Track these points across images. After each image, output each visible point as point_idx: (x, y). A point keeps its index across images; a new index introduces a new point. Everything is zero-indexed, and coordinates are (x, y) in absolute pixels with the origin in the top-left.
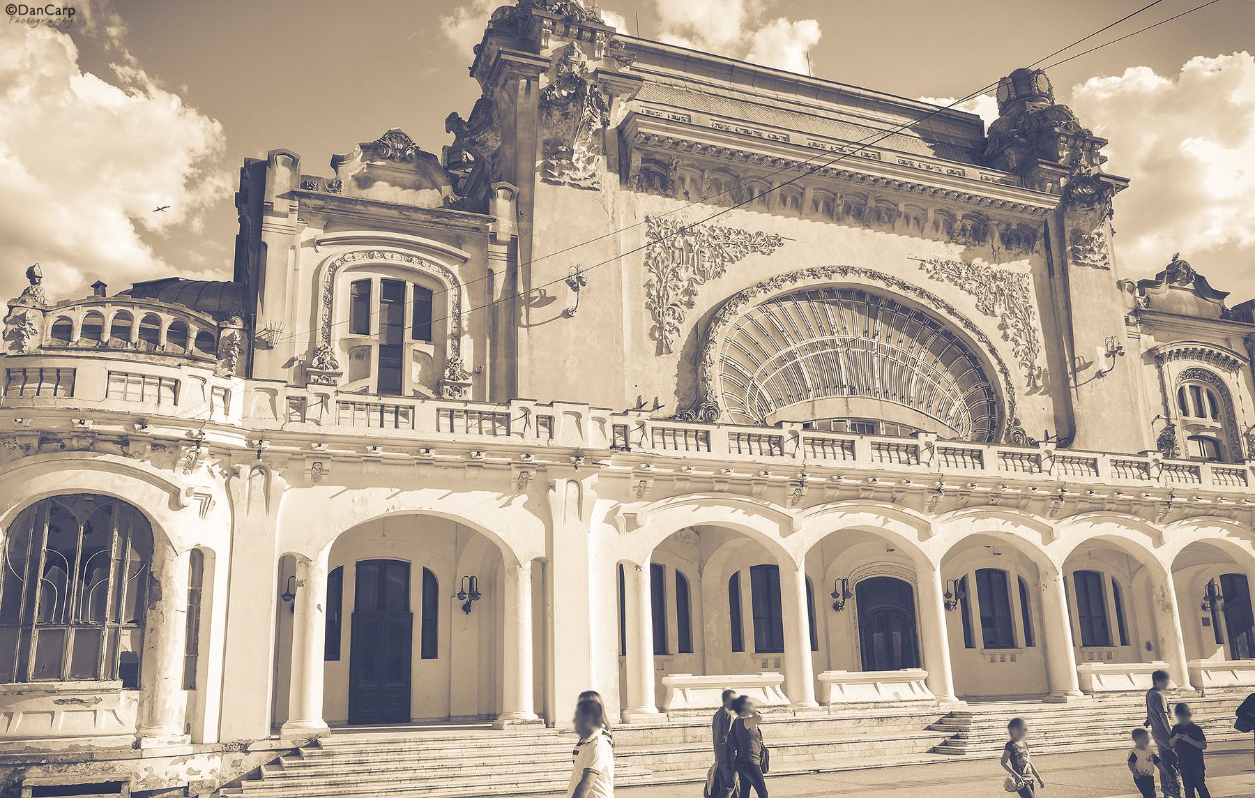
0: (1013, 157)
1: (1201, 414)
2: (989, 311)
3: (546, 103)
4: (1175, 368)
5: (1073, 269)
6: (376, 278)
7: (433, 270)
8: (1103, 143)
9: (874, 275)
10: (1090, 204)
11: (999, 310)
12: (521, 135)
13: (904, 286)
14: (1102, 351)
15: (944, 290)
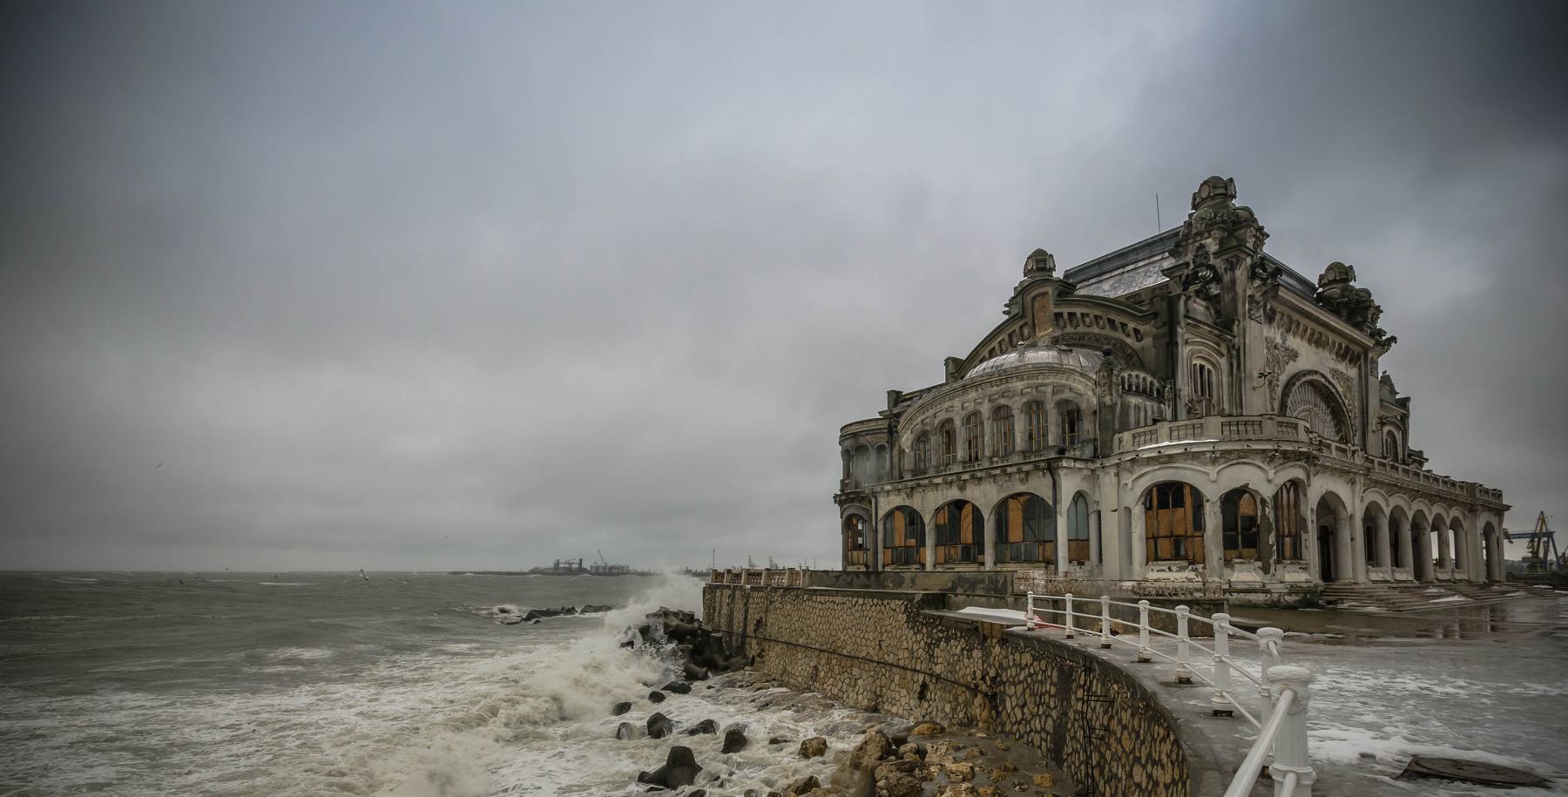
0: (1344, 312)
6: (1198, 362)
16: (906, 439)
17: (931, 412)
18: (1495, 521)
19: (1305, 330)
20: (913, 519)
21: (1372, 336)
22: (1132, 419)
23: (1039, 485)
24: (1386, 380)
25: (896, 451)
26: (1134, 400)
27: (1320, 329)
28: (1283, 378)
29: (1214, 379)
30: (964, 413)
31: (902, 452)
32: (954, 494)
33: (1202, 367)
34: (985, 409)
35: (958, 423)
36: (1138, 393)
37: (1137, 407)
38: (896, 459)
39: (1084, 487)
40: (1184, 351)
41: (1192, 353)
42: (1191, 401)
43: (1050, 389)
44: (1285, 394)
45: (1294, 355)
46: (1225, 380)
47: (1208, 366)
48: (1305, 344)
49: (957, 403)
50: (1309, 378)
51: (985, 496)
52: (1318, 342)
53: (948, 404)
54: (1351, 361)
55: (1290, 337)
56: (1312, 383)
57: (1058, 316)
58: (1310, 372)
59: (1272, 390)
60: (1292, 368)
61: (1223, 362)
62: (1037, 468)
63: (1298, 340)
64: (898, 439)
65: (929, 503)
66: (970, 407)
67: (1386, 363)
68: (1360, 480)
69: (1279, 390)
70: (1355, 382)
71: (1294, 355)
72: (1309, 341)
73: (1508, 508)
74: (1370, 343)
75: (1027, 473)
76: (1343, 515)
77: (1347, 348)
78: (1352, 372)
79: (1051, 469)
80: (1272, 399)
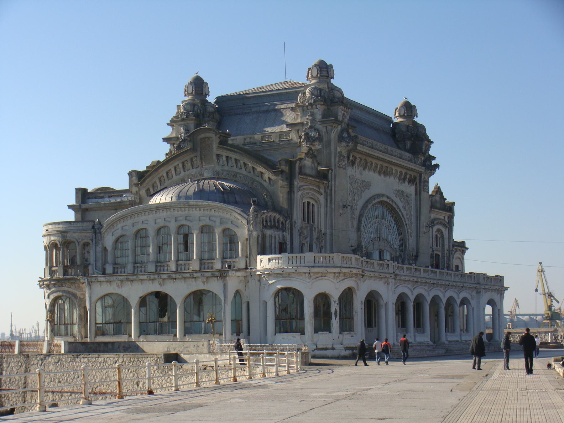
0: (408, 144)
1: (437, 246)
2: (404, 208)
3: (341, 139)
4: (435, 228)
5: (422, 192)
6: (306, 200)
7: (316, 198)
8: (433, 142)
9: (388, 197)
10: (431, 170)
11: (407, 208)
12: (332, 148)
13: (393, 201)
14: (425, 224)
15: (397, 200)
16: (109, 241)
17: (129, 222)
18: (496, 297)
19: (376, 167)
20: (122, 304)
21: (423, 164)
22: (268, 244)
23: (215, 286)
24: (438, 190)
25: (99, 249)
26: (268, 232)
27: (386, 165)
28: (360, 203)
29: (316, 210)
30: (157, 226)
31: (105, 249)
32: (155, 287)
33: (308, 203)
34: (173, 226)
35: (152, 233)
36: (271, 227)
37: (271, 236)
38: (99, 255)
39: (241, 287)
40: (298, 195)
41: (303, 197)
42: (302, 228)
43: (218, 220)
44: (361, 216)
45: (368, 185)
46: (322, 210)
47: (312, 202)
48: (376, 175)
49: (150, 218)
50: (377, 200)
51: (178, 291)
52: (385, 173)
53: (143, 218)
54: (409, 182)
55: (366, 171)
56: (381, 203)
57: (218, 156)
58: (379, 195)
59: (353, 211)
60: (367, 195)
61: (322, 198)
62: (214, 276)
63: (372, 173)
64: (102, 238)
65: (133, 292)
66: (161, 223)
67: (433, 181)
68: (392, 281)
69: (357, 212)
70: (413, 197)
71: (368, 185)
72: (380, 173)
73: (506, 289)
74: (422, 169)
75: (208, 278)
76: (382, 303)
77: (406, 174)
78: (411, 189)
79: (222, 275)
80: (352, 218)
